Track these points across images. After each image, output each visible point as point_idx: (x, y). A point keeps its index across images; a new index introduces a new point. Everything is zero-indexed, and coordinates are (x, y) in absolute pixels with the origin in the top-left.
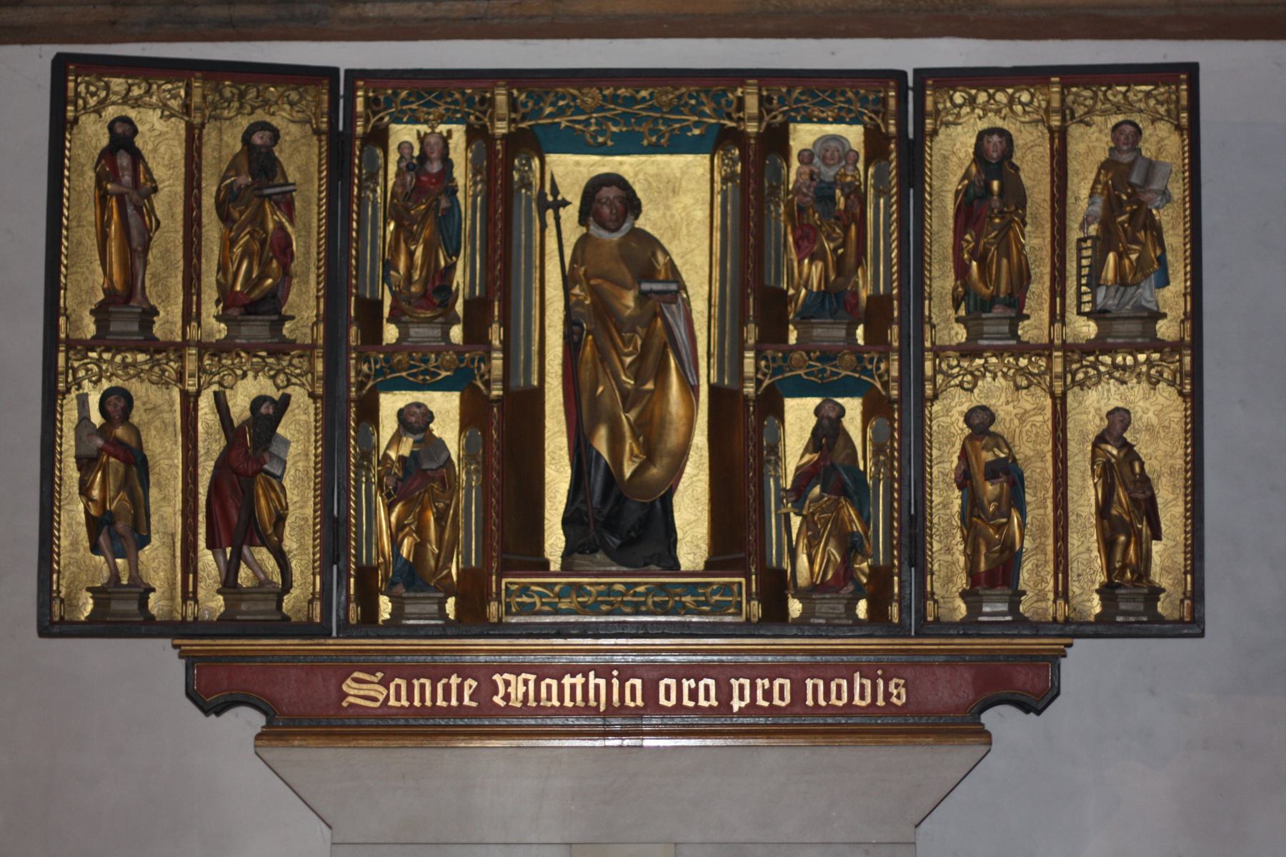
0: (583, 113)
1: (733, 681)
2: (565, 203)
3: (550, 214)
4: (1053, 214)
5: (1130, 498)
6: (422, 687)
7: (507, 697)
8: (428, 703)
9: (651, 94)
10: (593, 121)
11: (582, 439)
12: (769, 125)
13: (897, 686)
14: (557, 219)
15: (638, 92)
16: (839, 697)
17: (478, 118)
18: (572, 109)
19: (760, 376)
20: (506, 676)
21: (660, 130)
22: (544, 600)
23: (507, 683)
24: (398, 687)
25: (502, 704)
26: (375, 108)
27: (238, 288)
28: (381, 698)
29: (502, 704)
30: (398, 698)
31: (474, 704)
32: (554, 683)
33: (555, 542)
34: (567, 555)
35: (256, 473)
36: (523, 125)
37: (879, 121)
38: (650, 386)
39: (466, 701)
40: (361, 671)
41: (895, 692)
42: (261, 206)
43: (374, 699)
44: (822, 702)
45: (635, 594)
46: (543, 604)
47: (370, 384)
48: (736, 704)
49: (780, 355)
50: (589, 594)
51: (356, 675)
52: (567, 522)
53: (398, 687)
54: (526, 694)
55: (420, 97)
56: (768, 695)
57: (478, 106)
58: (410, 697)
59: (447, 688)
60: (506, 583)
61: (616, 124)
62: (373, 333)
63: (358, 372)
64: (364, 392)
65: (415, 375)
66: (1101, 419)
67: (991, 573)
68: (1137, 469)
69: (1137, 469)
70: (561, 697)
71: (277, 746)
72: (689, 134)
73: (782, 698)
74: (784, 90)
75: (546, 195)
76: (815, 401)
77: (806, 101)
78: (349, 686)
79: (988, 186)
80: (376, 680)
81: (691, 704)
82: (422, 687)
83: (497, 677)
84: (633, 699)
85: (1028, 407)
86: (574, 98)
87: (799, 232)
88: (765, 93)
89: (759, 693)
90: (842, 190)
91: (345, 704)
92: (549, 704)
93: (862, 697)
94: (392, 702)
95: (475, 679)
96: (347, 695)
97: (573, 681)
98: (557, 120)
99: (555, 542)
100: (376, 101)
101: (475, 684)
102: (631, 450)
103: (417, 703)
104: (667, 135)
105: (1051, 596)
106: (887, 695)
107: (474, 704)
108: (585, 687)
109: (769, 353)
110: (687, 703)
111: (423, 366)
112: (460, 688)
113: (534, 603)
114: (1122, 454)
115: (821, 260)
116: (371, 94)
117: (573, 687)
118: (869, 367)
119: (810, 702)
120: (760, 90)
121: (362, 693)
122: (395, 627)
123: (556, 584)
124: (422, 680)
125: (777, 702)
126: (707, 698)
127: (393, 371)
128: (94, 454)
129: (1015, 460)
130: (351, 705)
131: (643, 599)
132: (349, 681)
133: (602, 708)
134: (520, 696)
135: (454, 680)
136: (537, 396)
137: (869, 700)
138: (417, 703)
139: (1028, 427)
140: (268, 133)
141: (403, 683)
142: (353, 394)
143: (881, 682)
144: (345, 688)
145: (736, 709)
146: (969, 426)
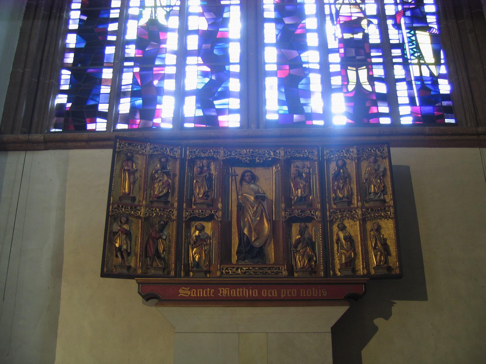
0: (242, 155)
1: (281, 290)
2: (237, 175)
3: (234, 177)
4: (356, 176)
5: (381, 244)
6: (200, 291)
7: (222, 294)
8: (202, 296)
9: (258, 151)
10: (244, 156)
11: (241, 231)
12: (286, 158)
13: (324, 291)
14: (235, 179)
15: (255, 150)
16: (309, 294)
17: (216, 156)
18: (239, 154)
19: (286, 216)
20: (222, 289)
21: (260, 159)
22: (232, 271)
23: (222, 290)
24: (193, 291)
25: (221, 296)
26: (192, 154)
27: (156, 193)
28: (189, 294)
29: (221, 296)
30: (193, 294)
31: (214, 296)
32: (235, 290)
33: (234, 258)
34: (237, 261)
35: (158, 239)
36: (228, 157)
37: (313, 157)
38: (258, 219)
39: (212, 295)
40: (186, 297)
41: (324, 293)
42: (163, 175)
43: (188, 294)
44: (305, 295)
45: (256, 270)
46: (231, 272)
47: (188, 217)
48: (282, 296)
49: (291, 211)
50: (243, 269)
51: (183, 288)
52: (238, 253)
53: (193, 291)
54: (227, 293)
55: (202, 151)
56: (290, 293)
57: (216, 153)
58: (197, 294)
59: (206, 292)
60: (222, 267)
61: (249, 157)
62: (190, 206)
63: (185, 214)
64: (187, 219)
65: (200, 215)
66: (371, 226)
67: (346, 263)
68: (382, 236)
69: (382, 236)
70: (236, 294)
71: (161, 306)
72: (267, 160)
73: (294, 294)
74: (290, 150)
75: (233, 173)
76: (298, 224)
77: (295, 152)
78: (180, 291)
79: (339, 171)
80: (188, 289)
81: (271, 296)
82: (200, 291)
83: (220, 289)
84: (255, 294)
85: (353, 224)
86: (239, 152)
87: (294, 184)
88: (285, 151)
89: (288, 292)
90: (305, 173)
91: (179, 296)
92: (233, 296)
93: (315, 294)
94: (192, 295)
95: (213, 289)
96: (180, 293)
97: (240, 290)
98: (236, 156)
99: (234, 258)
100: (192, 152)
101: (213, 290)
102: (254, 234)
103: (199, 295)
104: (262, 160)
105: (362, 270)
106: (322, 293)
107: (214, 296)
108: (243, 291)
109: (288, 210)
110: (269, 295)
111: (202, 213)
112: (210, 291)
113: (229, 272)
114: (377, 234)
115: (300, 189)
116: (191, 150)
117: (239, 291)
118: (313, 213)
119: (302, 295)
120: (284, 150)
121: (183, 293)
122: (193, 277)
123: (235, 267)
124: (200, 290)
125: (293, 295)
126: (275, 294)
127: (194, 214)
128: (118, 231)
129: (351, 235)
130: (181, 296)
131: (257, 271)
132: (181, 289)
133: (247, 297)
134: (226, 293)
135: (208, 290)
136: (230, 223)
137: (317, 295)
138: (199, 295)
139: (353, 229)
140: (165, 159)
141: (195, 290)
142: (184, 220)
143: (320, 290)
144: (180, 292)
145: (282, 297)
146: (338, 228)
